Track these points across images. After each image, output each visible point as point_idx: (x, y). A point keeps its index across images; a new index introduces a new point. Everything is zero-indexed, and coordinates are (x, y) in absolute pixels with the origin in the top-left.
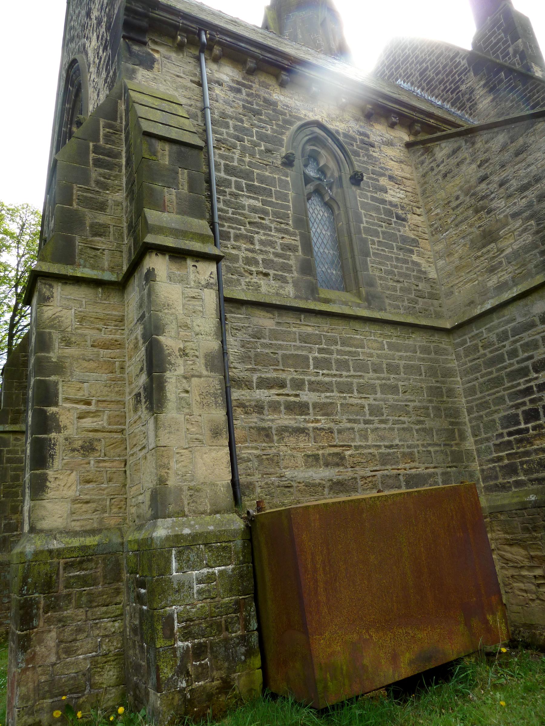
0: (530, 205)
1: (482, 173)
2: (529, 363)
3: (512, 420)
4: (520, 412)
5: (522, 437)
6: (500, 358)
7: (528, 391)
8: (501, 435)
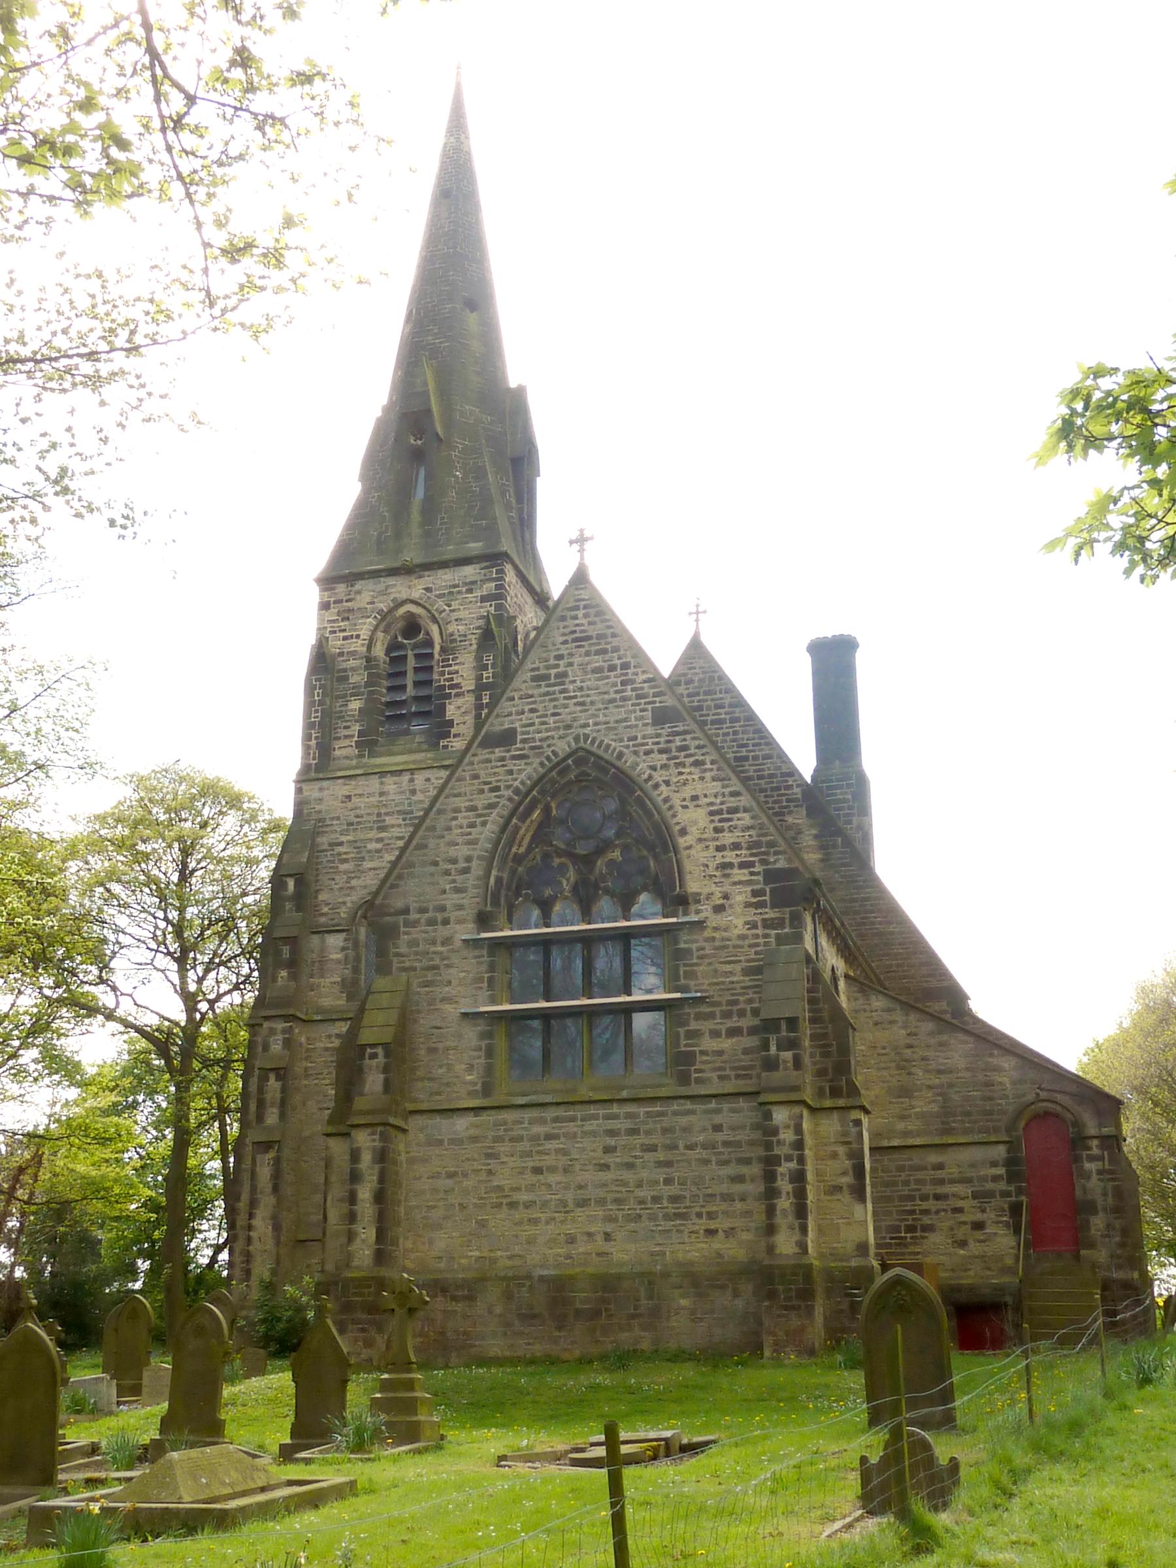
0: (941, 1086)
1: (909, 1041)
2: (917, 1193)
3: (897, 1229)
4: (903, 1224)
5: (902, 1242)
6: (895, 1184)
7: (913, 1212)
8: (885, 1238)
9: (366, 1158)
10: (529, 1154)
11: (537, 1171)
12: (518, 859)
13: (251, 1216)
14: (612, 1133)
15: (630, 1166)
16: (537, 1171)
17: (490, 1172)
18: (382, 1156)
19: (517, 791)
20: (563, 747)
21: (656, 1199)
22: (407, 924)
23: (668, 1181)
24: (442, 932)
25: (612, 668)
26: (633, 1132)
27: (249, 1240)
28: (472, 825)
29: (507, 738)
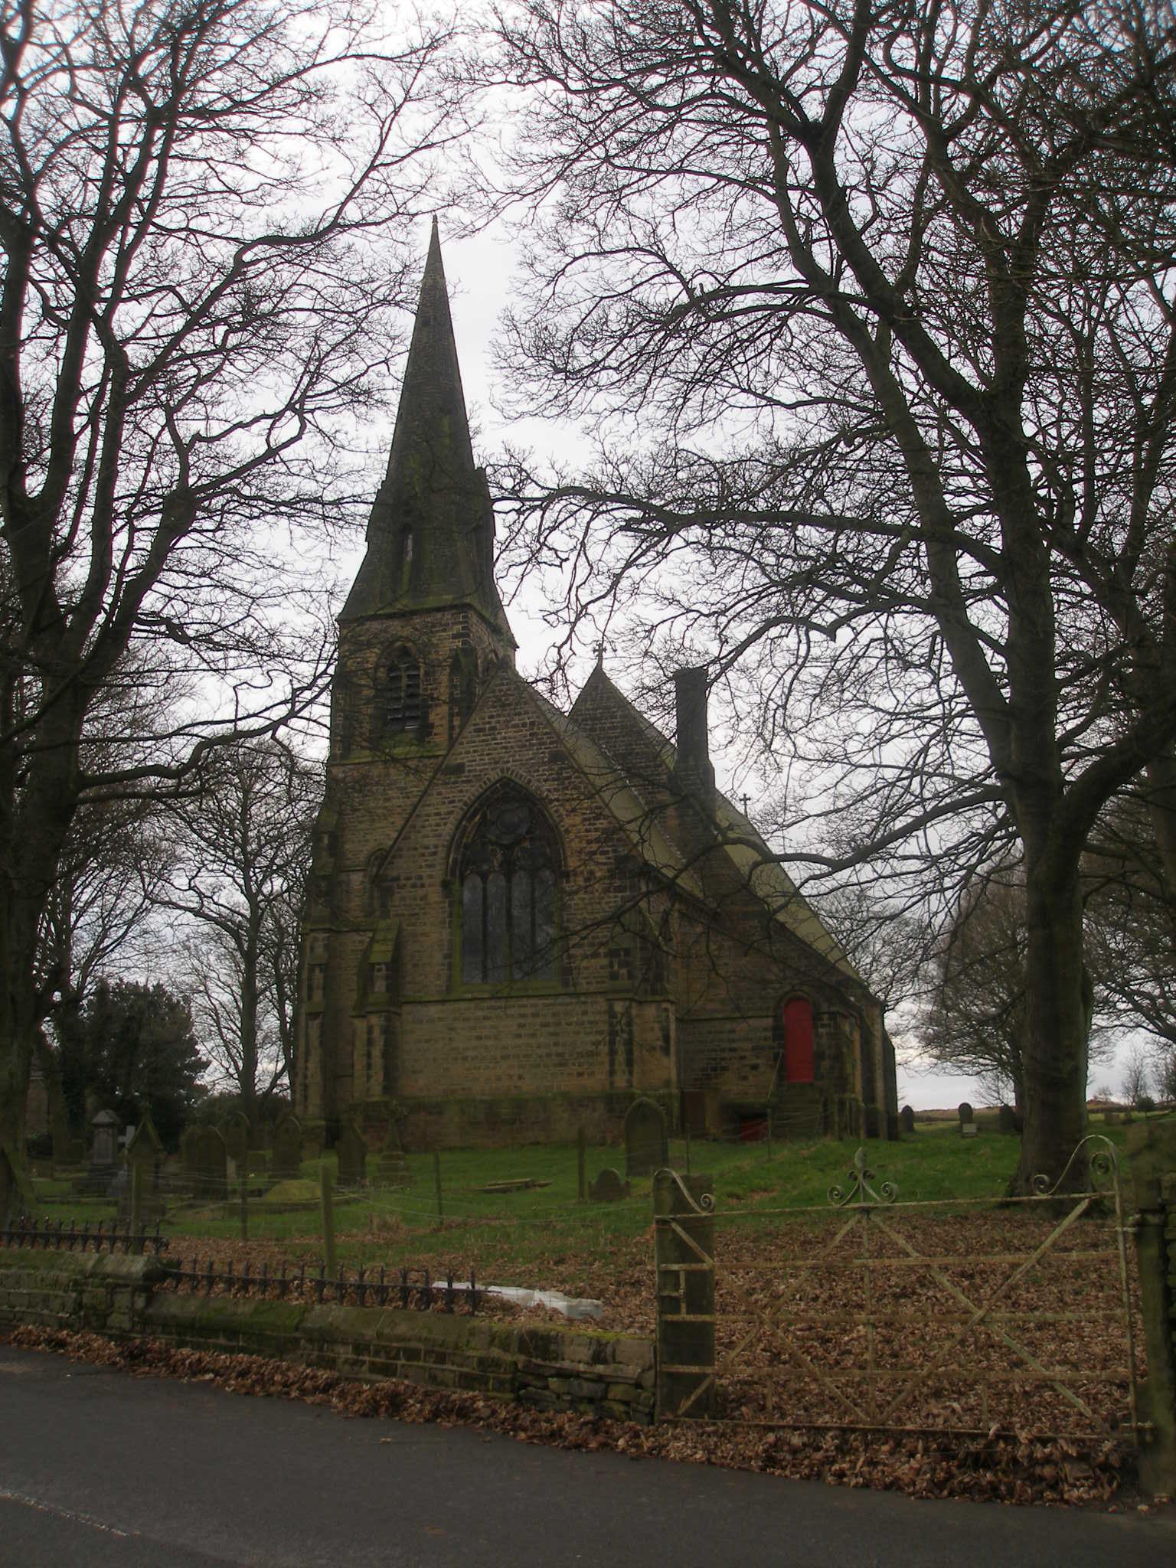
9: (376, 1032)
10: (474, 1028)
11: (479, 1038)
12: (466, 847)
13: (306, 1061)
14: (523, 1016)
15: (533, 1035)
16: (479, 1038)
17: (451, 1039)
18: (387, 1031)
19: (465, 804)
20: (494, 776)
21: (549, 1055)
22: (399, 887)
23: (556, 1044)
24: (421, 892)
25: (524, 725)
26: (535, 1015)
27: (306, 1077)
28: (438, 825)
29: (459, 769)
